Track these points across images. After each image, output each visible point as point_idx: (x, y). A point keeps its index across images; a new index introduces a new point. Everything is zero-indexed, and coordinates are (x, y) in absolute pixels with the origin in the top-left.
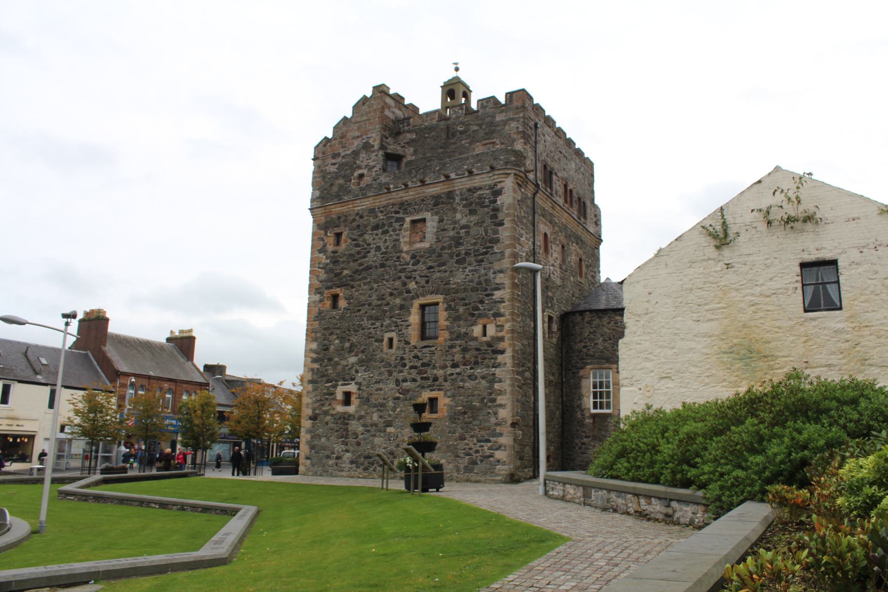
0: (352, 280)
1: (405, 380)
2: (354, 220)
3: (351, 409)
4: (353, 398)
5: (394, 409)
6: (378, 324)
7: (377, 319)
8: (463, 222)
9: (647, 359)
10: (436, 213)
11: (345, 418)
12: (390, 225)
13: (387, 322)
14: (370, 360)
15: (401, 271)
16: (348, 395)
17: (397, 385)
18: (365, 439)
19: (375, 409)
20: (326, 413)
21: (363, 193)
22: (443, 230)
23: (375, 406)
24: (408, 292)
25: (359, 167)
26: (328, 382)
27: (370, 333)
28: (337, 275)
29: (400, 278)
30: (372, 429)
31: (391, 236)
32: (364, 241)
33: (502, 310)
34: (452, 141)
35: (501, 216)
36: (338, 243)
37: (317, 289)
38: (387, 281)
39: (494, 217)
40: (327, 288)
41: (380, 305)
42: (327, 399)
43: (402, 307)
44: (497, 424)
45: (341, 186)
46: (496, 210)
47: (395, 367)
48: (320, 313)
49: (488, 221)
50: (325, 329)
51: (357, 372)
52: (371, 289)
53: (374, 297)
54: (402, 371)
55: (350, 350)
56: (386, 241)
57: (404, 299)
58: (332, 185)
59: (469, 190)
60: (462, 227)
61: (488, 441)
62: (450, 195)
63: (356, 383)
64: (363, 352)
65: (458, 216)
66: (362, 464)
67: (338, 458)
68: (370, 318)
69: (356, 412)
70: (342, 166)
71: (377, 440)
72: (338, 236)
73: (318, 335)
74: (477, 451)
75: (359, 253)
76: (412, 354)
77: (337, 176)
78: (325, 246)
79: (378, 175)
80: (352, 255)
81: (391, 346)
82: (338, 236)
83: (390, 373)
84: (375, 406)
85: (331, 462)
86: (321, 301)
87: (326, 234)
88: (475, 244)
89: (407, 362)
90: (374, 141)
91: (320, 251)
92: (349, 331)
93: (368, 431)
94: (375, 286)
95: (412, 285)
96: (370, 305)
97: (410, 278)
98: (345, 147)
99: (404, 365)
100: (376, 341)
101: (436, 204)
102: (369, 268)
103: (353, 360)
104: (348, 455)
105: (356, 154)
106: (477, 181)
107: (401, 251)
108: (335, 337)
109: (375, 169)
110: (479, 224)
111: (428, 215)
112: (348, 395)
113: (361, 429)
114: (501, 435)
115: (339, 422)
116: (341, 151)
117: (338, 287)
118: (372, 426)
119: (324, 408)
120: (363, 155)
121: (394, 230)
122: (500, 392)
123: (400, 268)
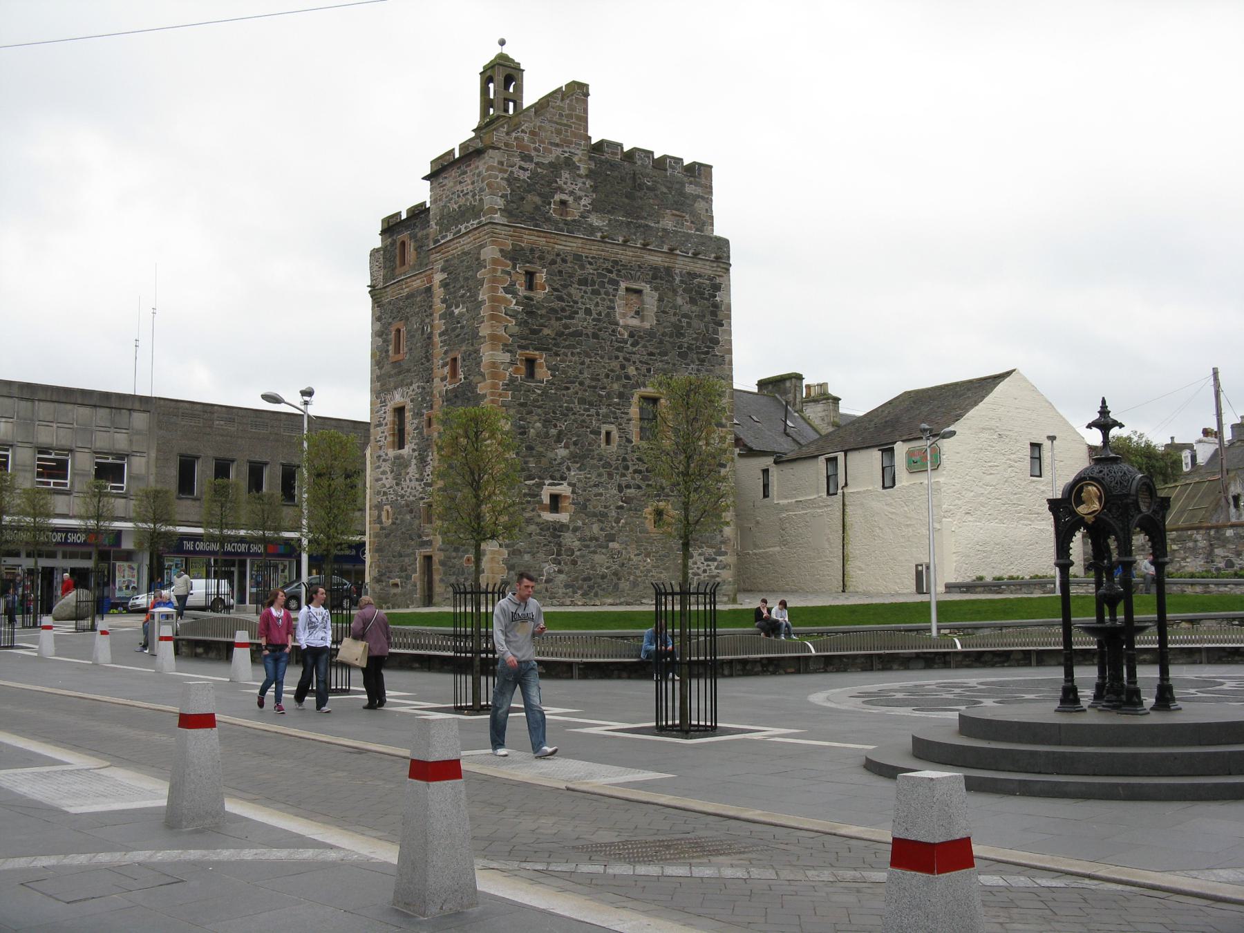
0: (555, 345)
1: (628, 487)
2: (553, 262)
3: (564, 517)
4: (565, 504)
5: (617, 521)
6: (593, 411)
7: (591, 404)
8: (687, 308)
9: (959, 499)
10: (656, 289)
11: (558, 528)
12: (602, 284)
13: (604, 410)
14: (584, 457)
15: (620, 349)
16: (555, 498)
17: (620, 491)
18: (583, 556)
19: (595, 519)
20: (529, 521)
21: (572, 227)
22: (664, 312)
23: (595, 515)
24: (627, 377)
25: (562, 191)
26: (530, 478)
27: (584, 421)
28: (534, 332)
29: (617, 358)
30: (591, 543)
31: (604, 300)
32: (570, 295)
33: (724, 421)
34: (639, 194)
35: (720, 316)
36: (530, 286)
37: (505, 345)
38: (602, 357)
39: (714, 314)
40: (520, 347)
41: (595, 387)
42: (528, 502)
43: (621, 395)
44: (722, 542)
45: (537, 208)
46: (716, 306)
47: (617, 468)
48: (512, 380)
49: (708, 318)
50: (521, 405)
51: (569, 469)
52: (583, 363)
53: (586, 375)
54: (623, 475)
55: (559, 439)
56: (597, 304)
57: (624, 386)
58: (523, 199)
59: (689, 274)
60: (685, 316)
61: (715, 560)
62: (668, 270)
63: (569, 484)
64: (575, 444)
65: (679, 301)
66: (581, 588)
67: (547, 581)
68: (582, 401)
69: (571, 521)
70: (534, 174)
71: (598, 558)
72: (530, 275)
73: (512, 412)
74: (705, 571)
75: (563, 310)
76: (636, 455)
77: (530, 188)
78: (513, 284)
79: (588, 211)
80: (553, 311)
81: (608, 442)
82: (530, 275)
83: (610, 475)
84: (595, 515)
85: (538, 587)
86: (512, 363)
87: (514, 267)
88: (696, 339)
89: (630, 464)
90: (580, 161)
91: (507, 290)
92: (554, 413)
93: (588, 546)
94: (587, 361)
95: (631, 370)
96: (581, 384)
97: (628, 360)
98: (538, 151)
99: (627, 468)
100: (591, 432)
101: (655, 277)
102: (578, 334)
103: (562, 452)
104: (562, 577)
105: (555, 167)
106: (697, 267)
107: (617, 324)
108: (536, 418)
109: (583, 202)
110: (701, 317)
111: (647, 288)
112: (555, 498)
113: (577, 543)
114: (726, 553)
115: (548, 534)
116: (533, 153)
117: (536, 349)
118: (591, 539)
119: (527, 515)
120: (565, 175)
121: (607, 293)
122: (727, 508)
123: (616, 345)
